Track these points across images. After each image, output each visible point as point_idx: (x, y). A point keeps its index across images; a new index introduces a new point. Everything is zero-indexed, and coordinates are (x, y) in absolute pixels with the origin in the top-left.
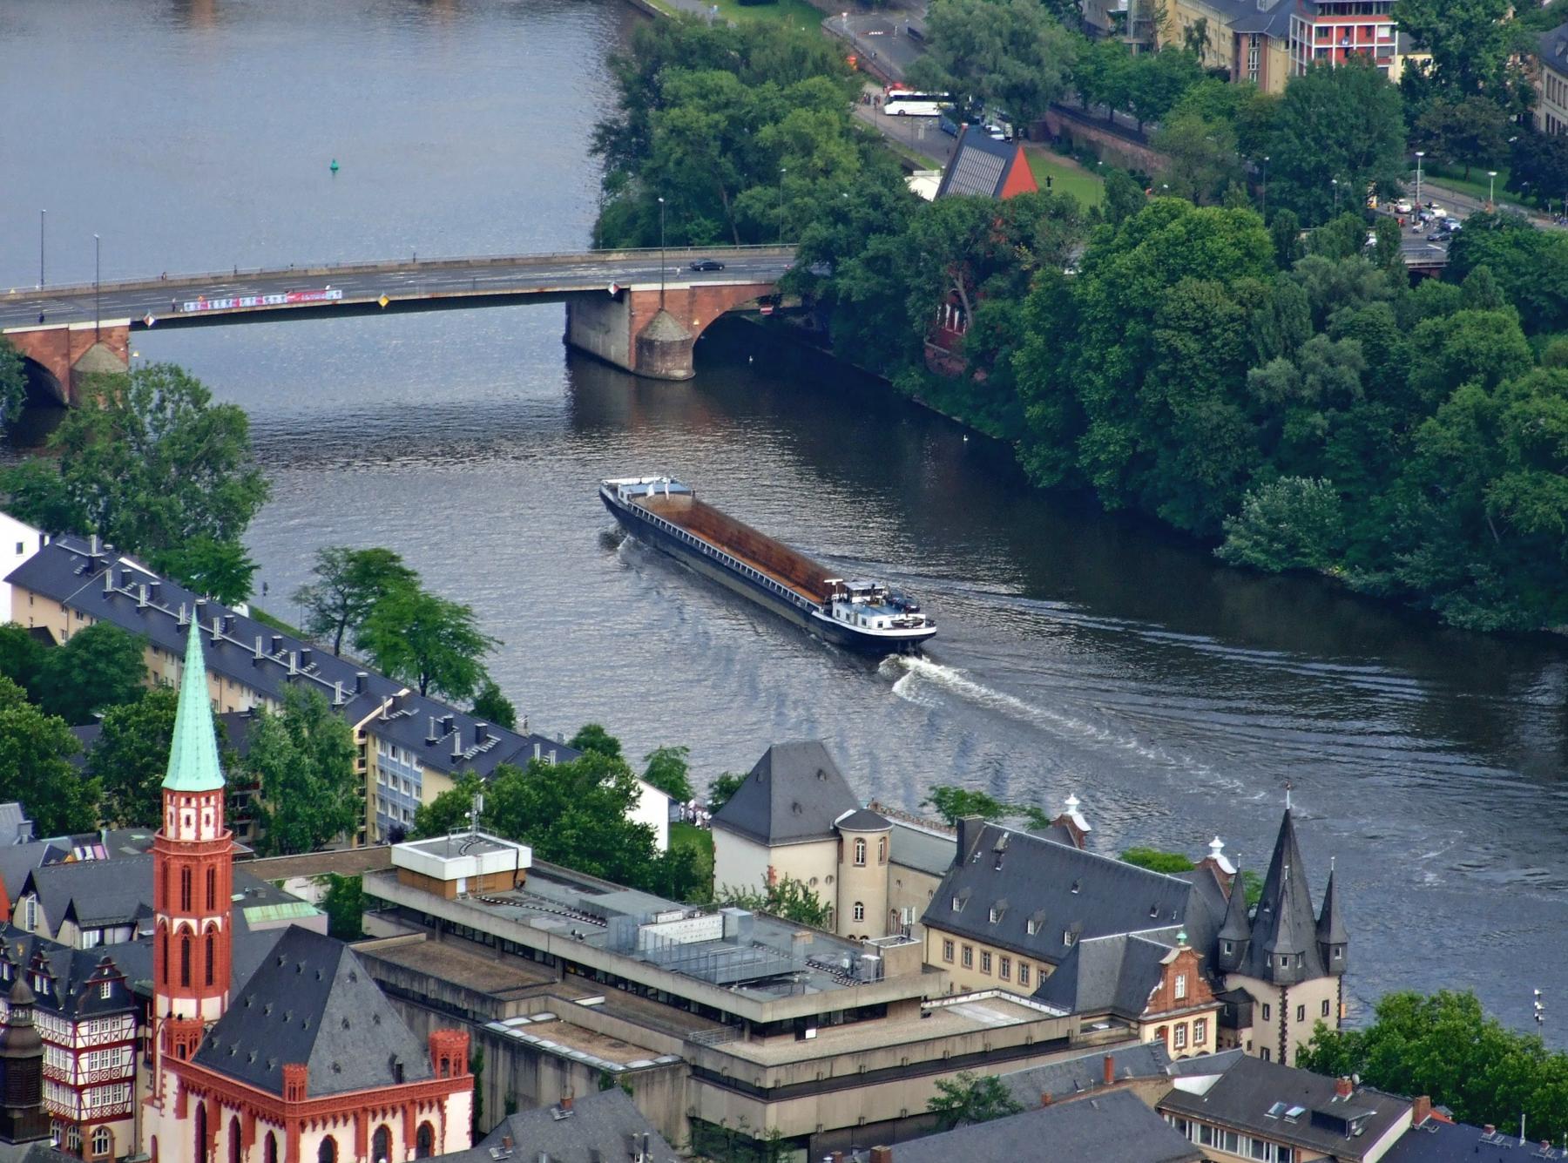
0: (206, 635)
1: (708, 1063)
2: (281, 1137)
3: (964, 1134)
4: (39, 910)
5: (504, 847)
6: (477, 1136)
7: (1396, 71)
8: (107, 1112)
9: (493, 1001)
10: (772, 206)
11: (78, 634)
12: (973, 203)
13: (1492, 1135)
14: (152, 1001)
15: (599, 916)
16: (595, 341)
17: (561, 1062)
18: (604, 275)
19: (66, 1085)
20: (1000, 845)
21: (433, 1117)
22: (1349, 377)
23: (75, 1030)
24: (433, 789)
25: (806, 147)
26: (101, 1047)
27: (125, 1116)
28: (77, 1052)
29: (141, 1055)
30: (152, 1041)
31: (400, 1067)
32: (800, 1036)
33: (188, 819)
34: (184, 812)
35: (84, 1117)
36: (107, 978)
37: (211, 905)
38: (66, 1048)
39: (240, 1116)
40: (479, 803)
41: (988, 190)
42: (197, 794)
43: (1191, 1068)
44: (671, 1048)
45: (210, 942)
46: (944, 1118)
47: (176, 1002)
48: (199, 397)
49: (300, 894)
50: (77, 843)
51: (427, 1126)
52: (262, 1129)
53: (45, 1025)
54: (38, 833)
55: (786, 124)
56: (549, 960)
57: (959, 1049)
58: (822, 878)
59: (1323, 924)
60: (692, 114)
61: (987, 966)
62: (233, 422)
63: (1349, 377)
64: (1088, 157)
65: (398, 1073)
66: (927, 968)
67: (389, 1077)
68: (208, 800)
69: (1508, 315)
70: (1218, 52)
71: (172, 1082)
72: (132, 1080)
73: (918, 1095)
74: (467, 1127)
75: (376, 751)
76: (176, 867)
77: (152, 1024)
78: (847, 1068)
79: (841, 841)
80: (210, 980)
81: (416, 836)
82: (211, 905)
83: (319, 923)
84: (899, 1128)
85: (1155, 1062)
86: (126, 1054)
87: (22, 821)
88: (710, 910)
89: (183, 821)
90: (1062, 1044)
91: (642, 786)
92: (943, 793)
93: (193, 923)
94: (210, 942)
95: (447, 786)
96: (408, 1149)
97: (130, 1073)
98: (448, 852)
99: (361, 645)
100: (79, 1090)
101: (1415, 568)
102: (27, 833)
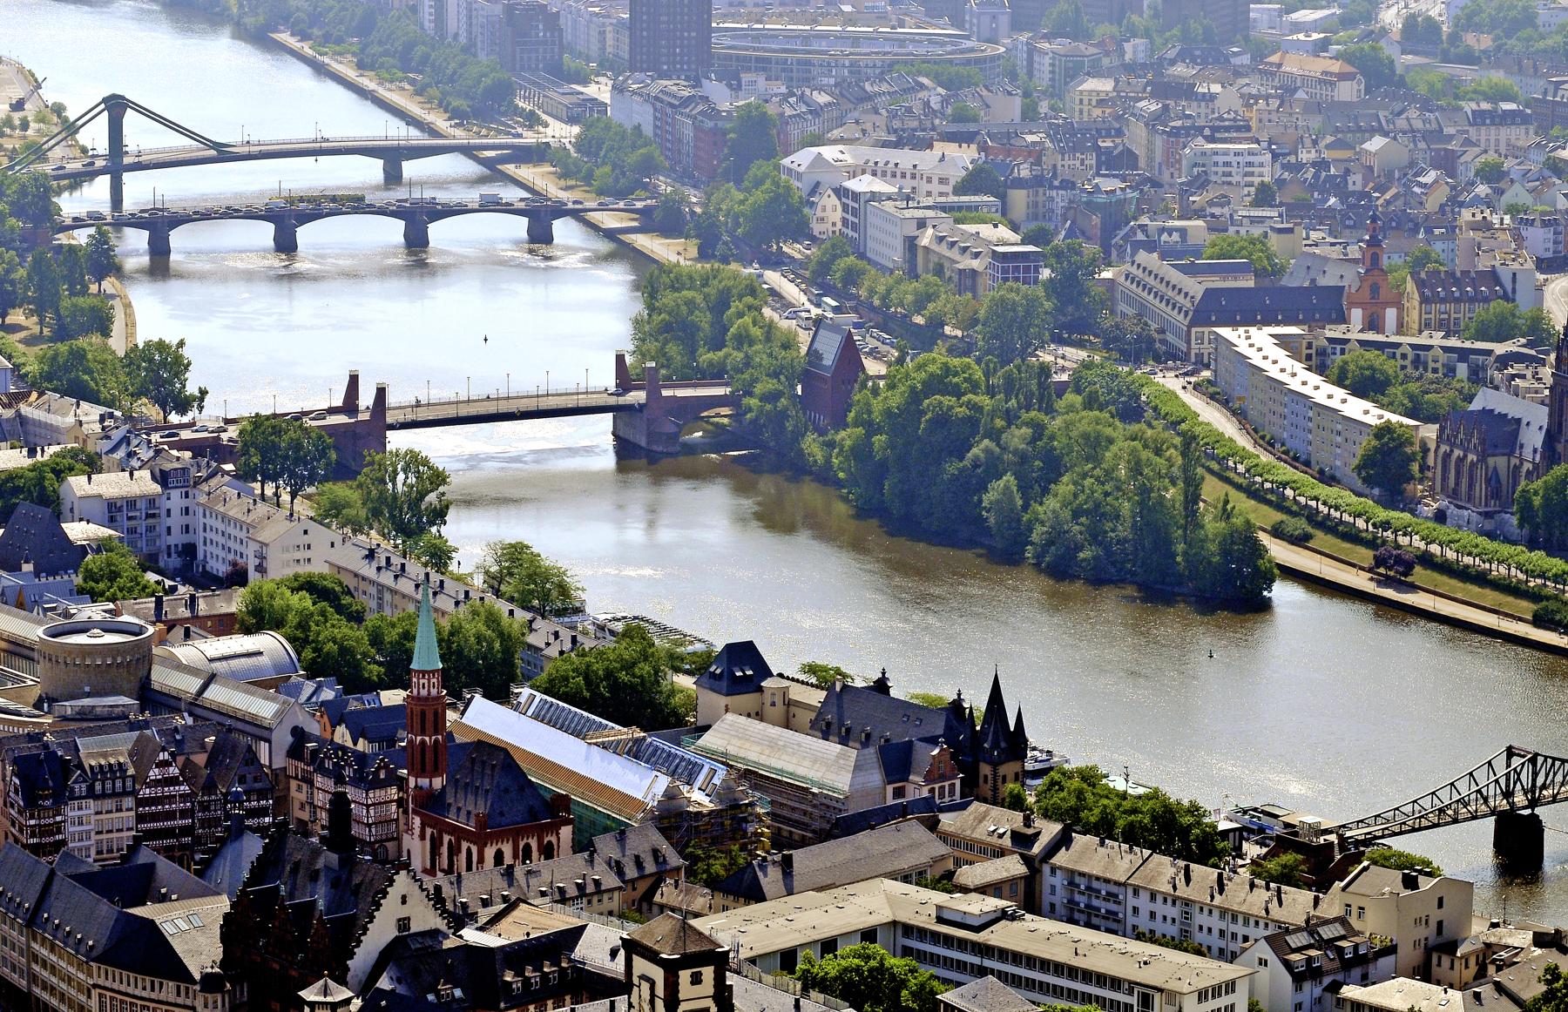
2: (474, 849)
21: (553, 839)
26: (380, 803)
27: (393, 839)
30: (407, 800)
34: (422, 681)
51: (550, 843)
52: (465, 845)
53: (351, 793)
71: (417, 821)
72: (397, 820)
77: (407, 792)
86: (394, 807)
93: (427, 739)
100: (369, 825)
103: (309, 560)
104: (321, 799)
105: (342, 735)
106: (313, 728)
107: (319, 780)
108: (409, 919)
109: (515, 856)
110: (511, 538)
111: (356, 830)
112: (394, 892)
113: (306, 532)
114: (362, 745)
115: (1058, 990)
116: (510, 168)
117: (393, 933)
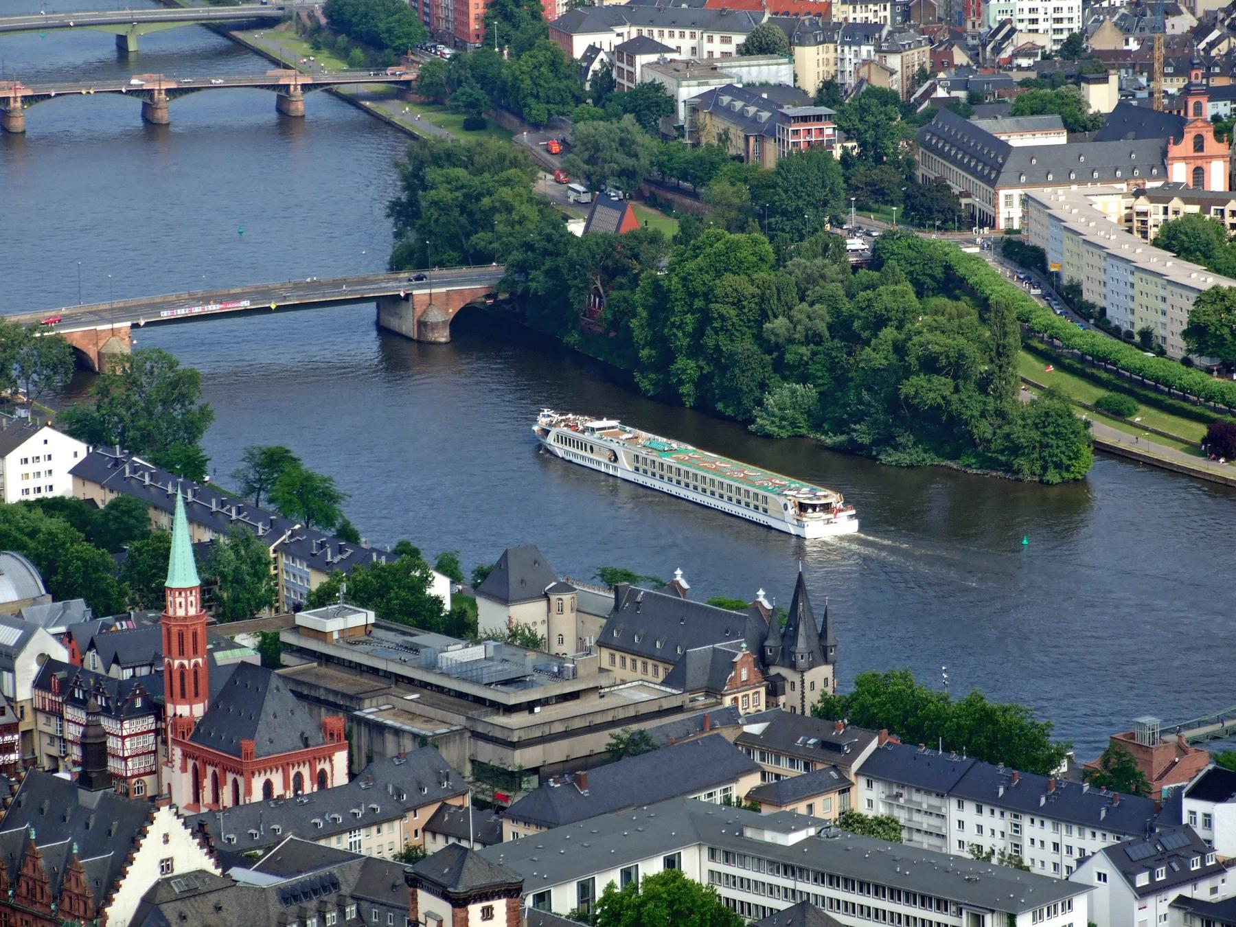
0: (185, 499)
1: (480, 729)
2: (241, 781)
3: (627, 762)
4: (98, 658)
5: (359, 612)
6: (352, 775)
7: (837, 153)
8: (142, 771)
9: (357, 699)
10: (490, 243)
11: (111, 502)
12: (605, 237)
13: (922, 749)
14: (164, 707)
15: (414, 649)
16: (393, 323)
17: (397, 732)
18: (398, 285)
19: (118, 756)
20: (639, 599)
21: (327, 767)
22: (821, 327)
23: (122, 725)
24: (317, 581)
25: (509, 209)
26: (136, 734)
28: (123, 738)
29: (159, 738)
30: (166, 730)
31: (306, 738)
32: (531, 711)
33: (180, 603)
34: (178, 600)
35: (129, 774)
36: (139, 695)
37: (195, 652)
38: (117, 736)
39: (217, 770)
40: (344, 587)
41: (611, 229)
42: (185, 590)
43: (752, 719)
44: (459, 721)
45: (196, 672)
46: (615, 754)
47: (178, 707)
48: (172, 365)
49: (244, 643)
50: (117, 620)
51: (323, 772)
53: (107, 724)
54: (95, 615)
55: (496, 196)
56: (388, 675)
57: (621, 714)
58: (539, 622)
59: (823, 635)
60: (443, 193)
61: (634, 667)
62: (192, 379)
63: (821, 327)
64: (665, 208)
65: (306, 742)
66: (601, 670)
67: (301, 745)
68: (191, 593)
69: (907, 287)
70: (736, 146)
71: (177, 753)
72: (155, 752)
73: (599, 742)
74: (346, 771)
75: (283, 561)
76: (175, 631)
77: (165, 720)
78: (558, 728)
79: (549, 600)
80: (196, 694)
81: (307, 608)
82: (195, 652)
83: (255, 659)
84: (589, 762)
85: (731, 716)
87: (85, 608)
88: (478, 643)
89: (178, 605)
90: (679, 709)
91: (435, 574)
92: (604, 570)
93: (186, 662)
94: (196, 672)
95: (324, 579)
96: (313, 784)
97: (154, 749)
98: (327, 616)
99: (271, 501)
100: (125, 759)
101: (863, 434)
102: (89, 615)
103: (50, 472)
104: (73, 732)
105: (92, 661)
106: (61, 654)
107: (70, 712)
108: (171, 859)
109: (286, 786)
110: (273, 443)
111: (113, 765)
112: (155, 831)
113: (46, 442)
114: (115, 671)
115: (881, 914)
116: (255, 38)
117: (154, 876)
